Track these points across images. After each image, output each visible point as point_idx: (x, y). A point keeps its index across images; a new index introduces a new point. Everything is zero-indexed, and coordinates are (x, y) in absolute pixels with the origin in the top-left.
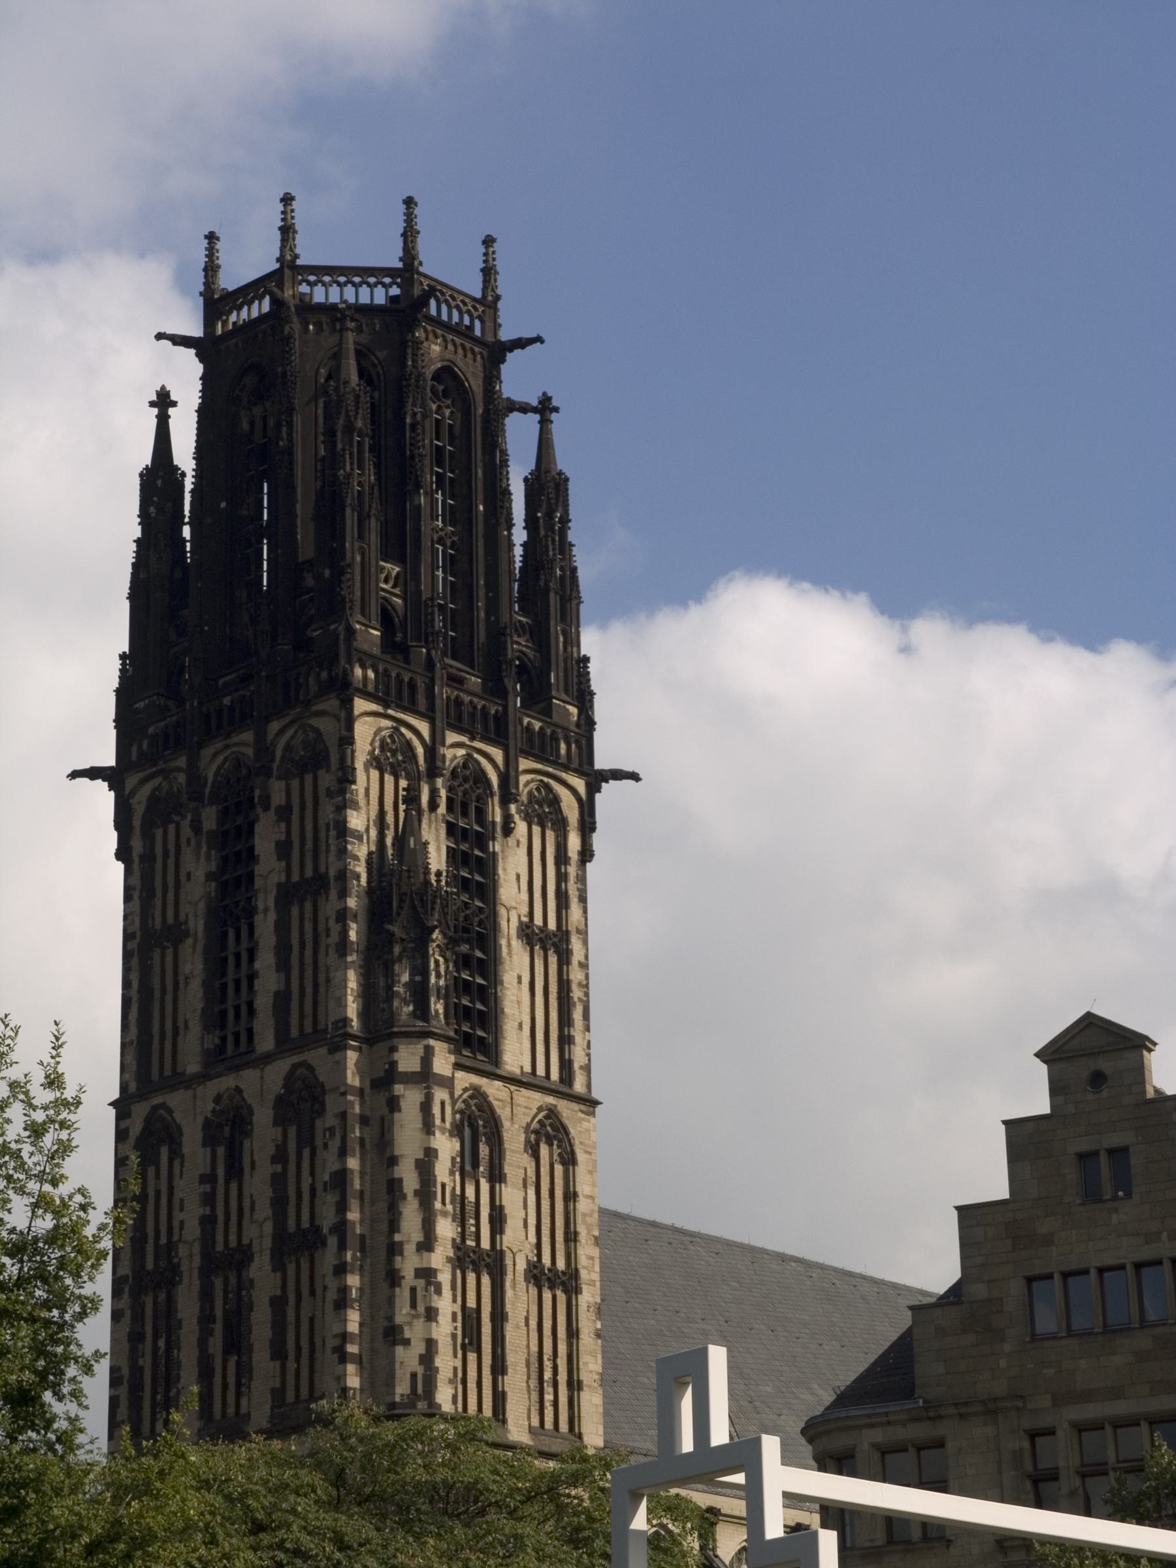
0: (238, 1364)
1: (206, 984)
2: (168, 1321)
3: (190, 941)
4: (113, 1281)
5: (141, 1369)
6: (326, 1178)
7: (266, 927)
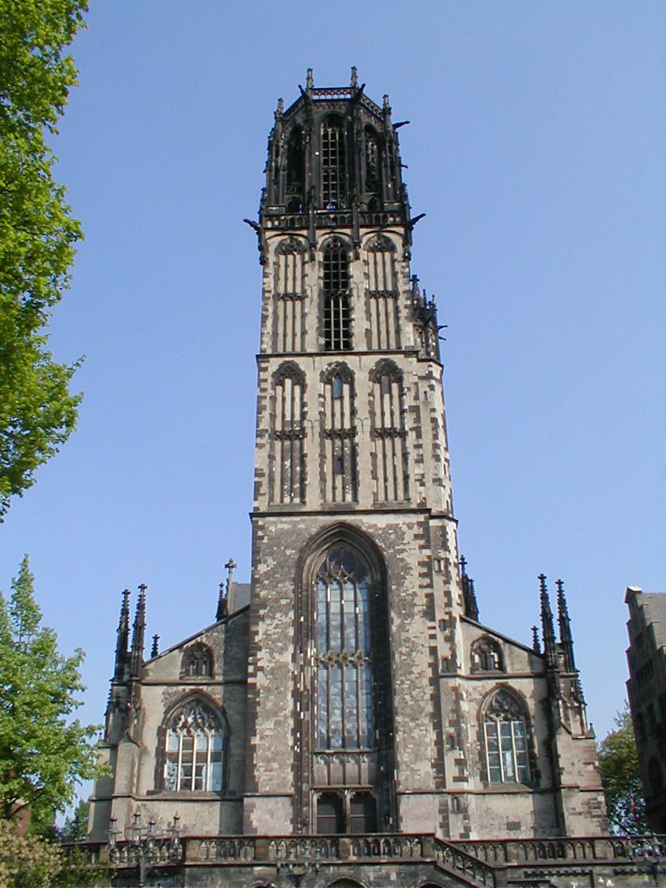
3: (307, 301)
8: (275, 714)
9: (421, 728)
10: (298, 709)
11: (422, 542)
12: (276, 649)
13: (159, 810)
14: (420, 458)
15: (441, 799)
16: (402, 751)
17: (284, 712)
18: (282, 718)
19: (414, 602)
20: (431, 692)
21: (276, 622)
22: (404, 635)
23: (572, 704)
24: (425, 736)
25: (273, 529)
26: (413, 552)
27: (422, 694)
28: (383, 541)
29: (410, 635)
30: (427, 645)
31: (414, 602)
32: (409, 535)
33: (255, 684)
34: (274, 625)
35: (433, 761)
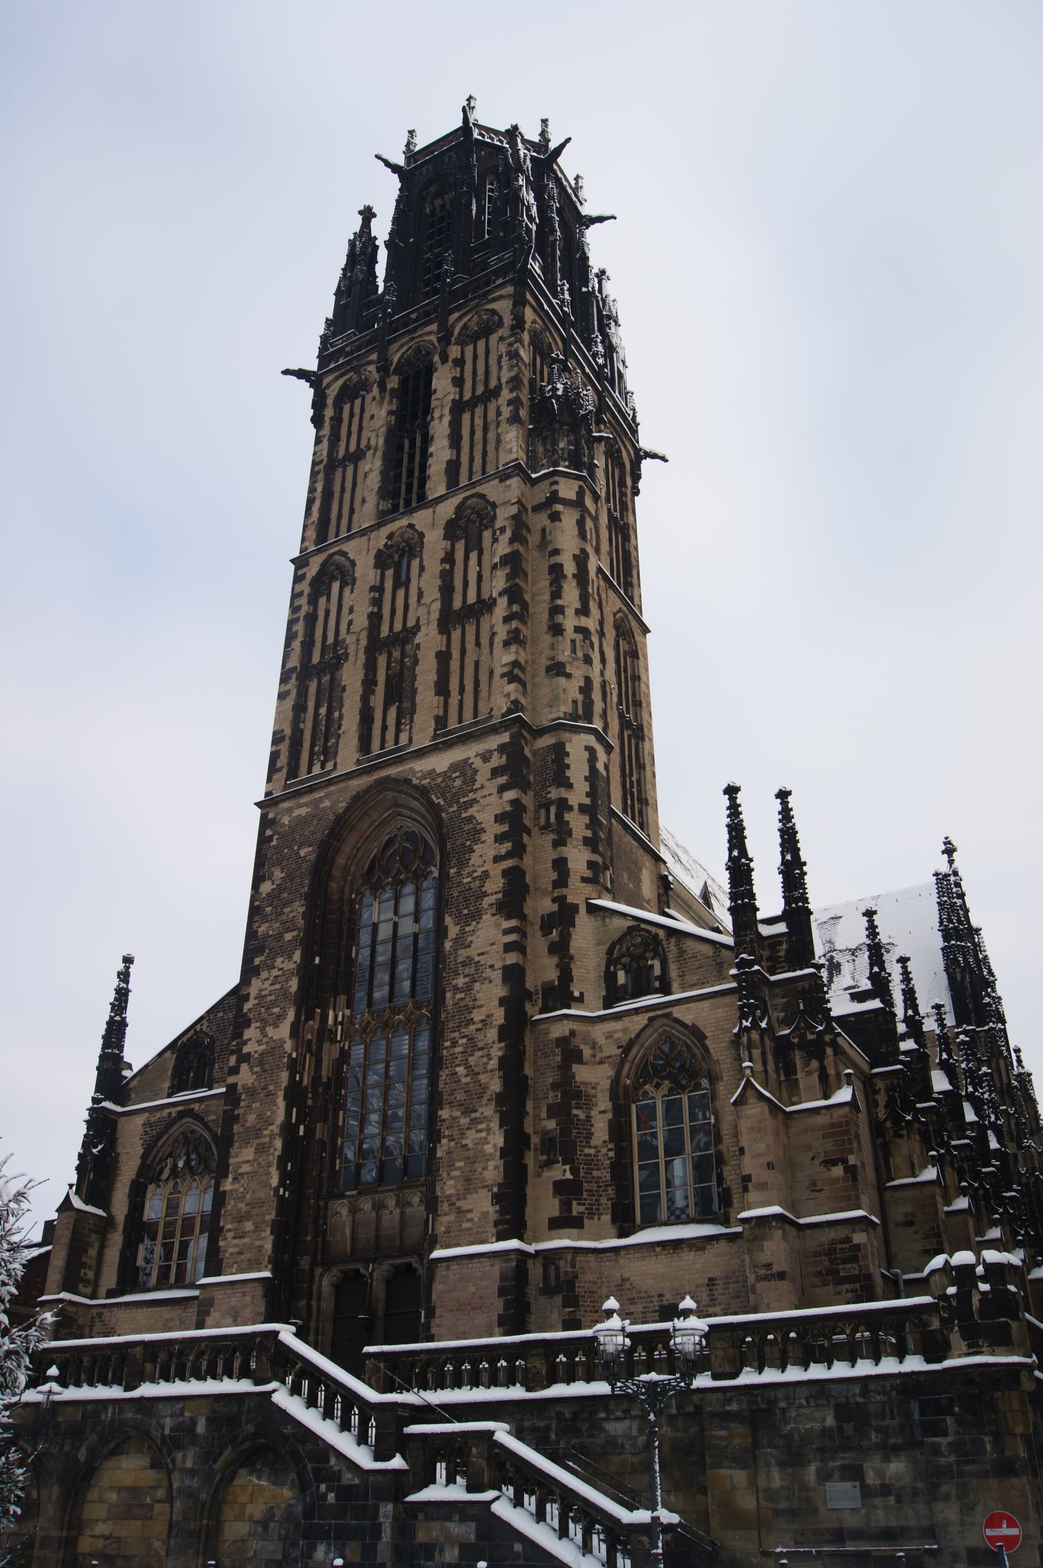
0: (399, 710)
1: (384, 474)
2: (332, 695)
4: (282, 674)
5: (302, 731)
6: (497, 560)
7: (440, 428)
8: (258, 1132)
9: (480, 1127)
10: (294, 1121)
11: (503, 780)
12: (270, 1020)
13: (116, 1324)
14: (512, 635)
15: (504, 1265)
16: (445, 1174)
17: (270, 1128)
18: (267, 1140)
19: (483, 889)
20: (500, 1053)
21: (275, 972)
22: (463, 954)
23: (802, 1037)
24: (485, 1141)
25: (286, 820)
26: (489, 800)
27: (485, 1060)
28: (443, 795)
29: (472, 952)
30: (498, 965)
31: (483, 889)
32: (482, 777)
33: (236, 1084)
34: (272, 978)
35: (495, 1189)
